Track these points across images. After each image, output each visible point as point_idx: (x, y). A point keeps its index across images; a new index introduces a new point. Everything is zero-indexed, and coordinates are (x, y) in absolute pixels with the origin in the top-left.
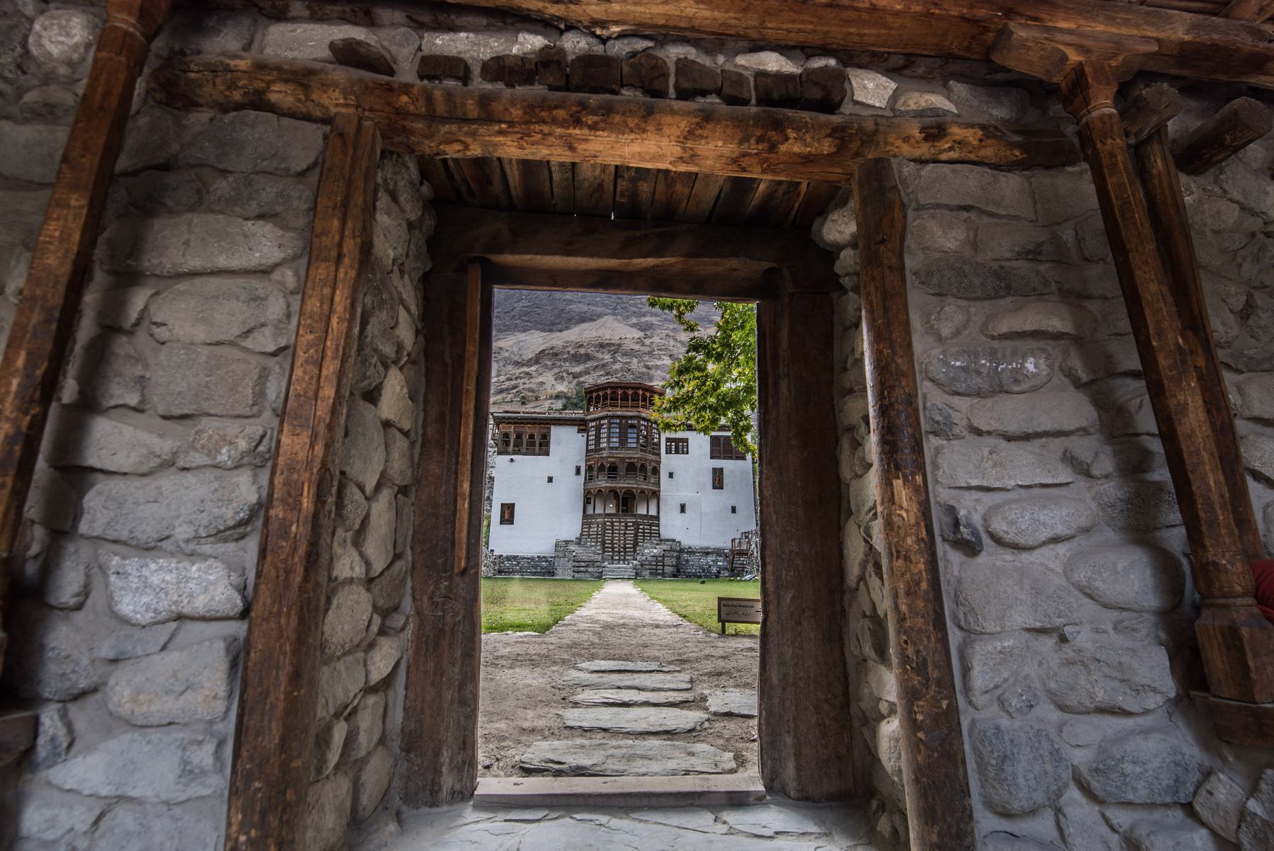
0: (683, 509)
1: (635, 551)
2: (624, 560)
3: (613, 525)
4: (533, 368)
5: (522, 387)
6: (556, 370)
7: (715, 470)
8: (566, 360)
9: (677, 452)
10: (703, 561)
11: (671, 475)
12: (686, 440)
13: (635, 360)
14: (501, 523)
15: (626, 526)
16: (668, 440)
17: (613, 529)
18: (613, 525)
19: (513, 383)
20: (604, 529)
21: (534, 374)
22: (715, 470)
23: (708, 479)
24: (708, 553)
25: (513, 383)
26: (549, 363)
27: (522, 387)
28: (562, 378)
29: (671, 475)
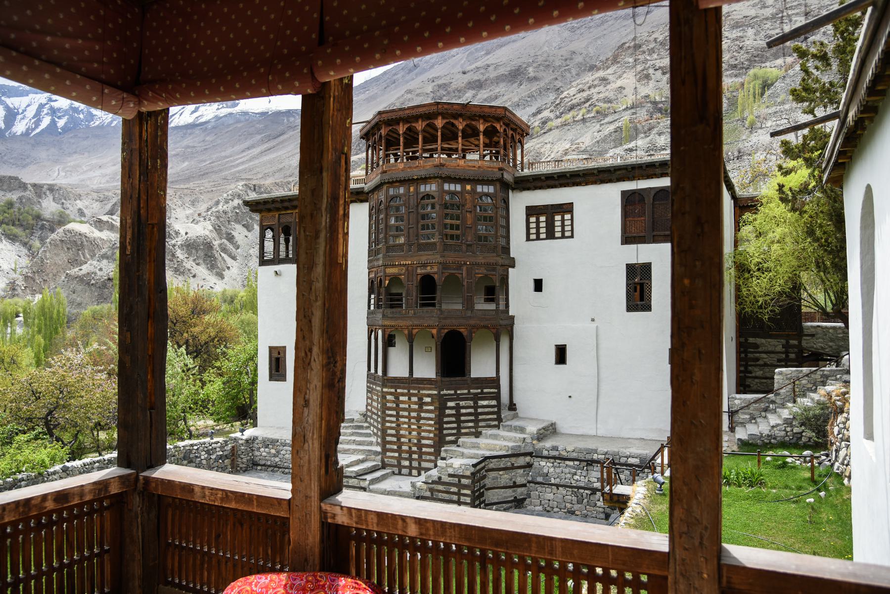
0: (561, 355)
1: (437, 453)
2: (420, 470)
3: (397, 402)
4: (610, 71)
5: (595, 97)
6: (639, 68)
7: (632, 270)
8: (651, 51)
9: (551, 235)
10: (580, 478)
11: (538, 285)
12: (567, 208)
13: (750, 32)
14: (271, 378)
15: (421, 404)
16: (532, 211)
17: (397, 409)
18: (397, 402)
19: (585, 94)
20: (384, 408)
21: (611, 78)
22: (632, 270)
23: (618, 288)
24: (591, 463)
25: (585, 94)
26: (631, 60)
27: (595, 97)
28: (648, 77)
29: (538, 285)
